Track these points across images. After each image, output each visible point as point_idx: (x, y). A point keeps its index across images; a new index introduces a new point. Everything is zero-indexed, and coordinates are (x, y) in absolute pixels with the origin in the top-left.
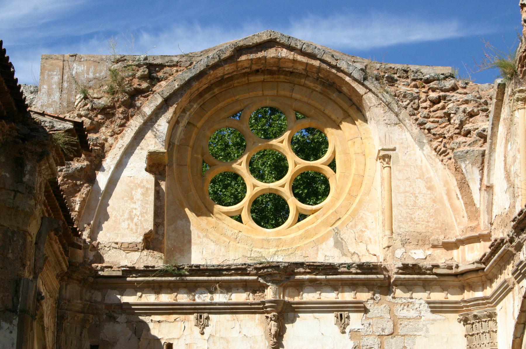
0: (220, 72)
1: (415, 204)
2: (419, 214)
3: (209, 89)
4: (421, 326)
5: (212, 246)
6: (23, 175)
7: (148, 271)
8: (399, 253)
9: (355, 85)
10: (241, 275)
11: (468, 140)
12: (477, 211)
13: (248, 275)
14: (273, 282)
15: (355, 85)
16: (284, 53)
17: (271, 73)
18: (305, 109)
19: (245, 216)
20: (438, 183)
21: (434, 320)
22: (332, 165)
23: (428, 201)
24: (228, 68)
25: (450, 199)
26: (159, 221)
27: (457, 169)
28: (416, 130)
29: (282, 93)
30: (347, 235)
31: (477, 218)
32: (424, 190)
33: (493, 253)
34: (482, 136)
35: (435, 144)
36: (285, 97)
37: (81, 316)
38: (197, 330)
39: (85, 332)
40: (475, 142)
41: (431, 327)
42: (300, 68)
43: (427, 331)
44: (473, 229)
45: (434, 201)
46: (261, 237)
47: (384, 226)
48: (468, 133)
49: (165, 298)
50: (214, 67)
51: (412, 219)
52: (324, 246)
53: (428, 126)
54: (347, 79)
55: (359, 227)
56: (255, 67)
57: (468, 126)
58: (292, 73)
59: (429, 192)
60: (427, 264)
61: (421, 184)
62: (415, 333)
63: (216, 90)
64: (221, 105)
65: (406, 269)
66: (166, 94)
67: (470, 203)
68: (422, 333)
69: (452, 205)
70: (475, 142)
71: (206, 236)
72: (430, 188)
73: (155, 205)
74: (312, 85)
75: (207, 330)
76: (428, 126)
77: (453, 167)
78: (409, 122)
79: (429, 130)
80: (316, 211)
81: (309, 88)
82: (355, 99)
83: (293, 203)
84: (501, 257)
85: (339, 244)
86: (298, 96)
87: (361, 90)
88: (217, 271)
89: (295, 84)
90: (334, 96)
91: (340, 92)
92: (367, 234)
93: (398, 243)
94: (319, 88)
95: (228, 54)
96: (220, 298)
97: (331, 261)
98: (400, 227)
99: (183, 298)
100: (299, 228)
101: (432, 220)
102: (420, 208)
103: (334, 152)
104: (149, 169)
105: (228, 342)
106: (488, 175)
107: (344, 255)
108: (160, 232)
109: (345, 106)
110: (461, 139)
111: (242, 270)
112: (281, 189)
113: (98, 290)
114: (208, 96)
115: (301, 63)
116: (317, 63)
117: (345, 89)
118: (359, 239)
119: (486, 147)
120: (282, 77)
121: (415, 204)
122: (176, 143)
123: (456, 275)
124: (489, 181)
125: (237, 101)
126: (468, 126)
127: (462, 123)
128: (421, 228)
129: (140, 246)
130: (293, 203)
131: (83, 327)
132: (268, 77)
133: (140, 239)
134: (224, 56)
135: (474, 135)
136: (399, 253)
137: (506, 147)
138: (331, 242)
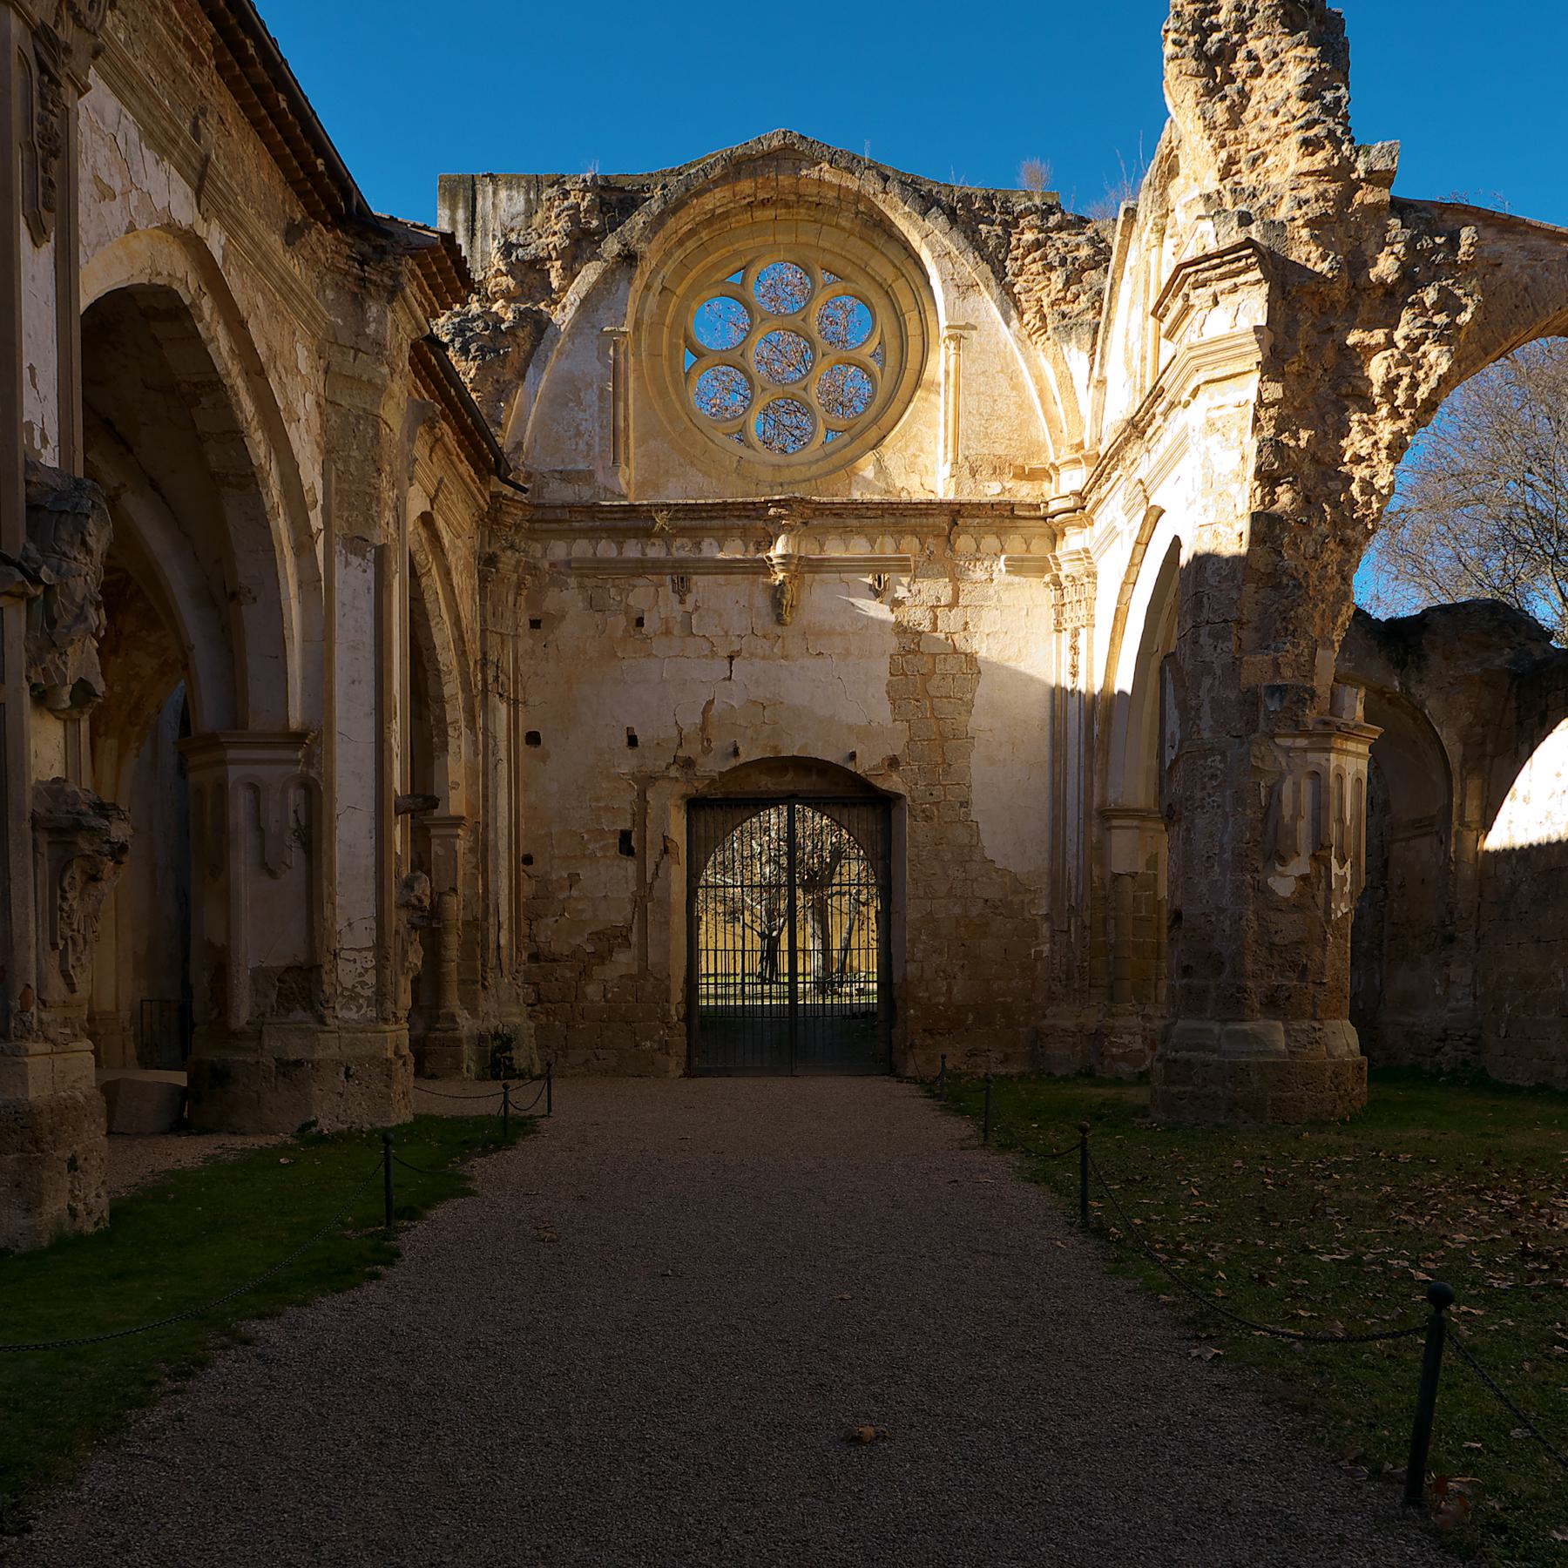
4: (991, 592)
21: (1009, 584)
23: (1012, 407)
25: (1043, 403)
29: (803, 239)
36: (807, 245)
38: (675, 598)
39: (522, 600)
41: (1004, 596)
43: (999, 600)
45: (1020, 407)
47: (946, 446)
59: (1014, 393)
62: (983, 603)
63: (704, 235)
64: (711, 259)
68: (993, 603)
69: (1046, 413)
71: (692, 464)
75: (690, 598)
81: (843, 229)
86: (828, 245)
89: (823, 224)
98: (968, 448)
101: (1016, 436)
106: (1102, 366)
113: (537, 540)
120: (803, 211)
124: (1100, 374)
125: (736, 252)
128: (999, 449)
131: (518, 594)
137: (1129, 314)
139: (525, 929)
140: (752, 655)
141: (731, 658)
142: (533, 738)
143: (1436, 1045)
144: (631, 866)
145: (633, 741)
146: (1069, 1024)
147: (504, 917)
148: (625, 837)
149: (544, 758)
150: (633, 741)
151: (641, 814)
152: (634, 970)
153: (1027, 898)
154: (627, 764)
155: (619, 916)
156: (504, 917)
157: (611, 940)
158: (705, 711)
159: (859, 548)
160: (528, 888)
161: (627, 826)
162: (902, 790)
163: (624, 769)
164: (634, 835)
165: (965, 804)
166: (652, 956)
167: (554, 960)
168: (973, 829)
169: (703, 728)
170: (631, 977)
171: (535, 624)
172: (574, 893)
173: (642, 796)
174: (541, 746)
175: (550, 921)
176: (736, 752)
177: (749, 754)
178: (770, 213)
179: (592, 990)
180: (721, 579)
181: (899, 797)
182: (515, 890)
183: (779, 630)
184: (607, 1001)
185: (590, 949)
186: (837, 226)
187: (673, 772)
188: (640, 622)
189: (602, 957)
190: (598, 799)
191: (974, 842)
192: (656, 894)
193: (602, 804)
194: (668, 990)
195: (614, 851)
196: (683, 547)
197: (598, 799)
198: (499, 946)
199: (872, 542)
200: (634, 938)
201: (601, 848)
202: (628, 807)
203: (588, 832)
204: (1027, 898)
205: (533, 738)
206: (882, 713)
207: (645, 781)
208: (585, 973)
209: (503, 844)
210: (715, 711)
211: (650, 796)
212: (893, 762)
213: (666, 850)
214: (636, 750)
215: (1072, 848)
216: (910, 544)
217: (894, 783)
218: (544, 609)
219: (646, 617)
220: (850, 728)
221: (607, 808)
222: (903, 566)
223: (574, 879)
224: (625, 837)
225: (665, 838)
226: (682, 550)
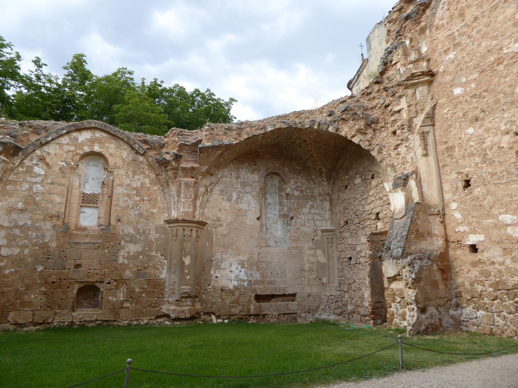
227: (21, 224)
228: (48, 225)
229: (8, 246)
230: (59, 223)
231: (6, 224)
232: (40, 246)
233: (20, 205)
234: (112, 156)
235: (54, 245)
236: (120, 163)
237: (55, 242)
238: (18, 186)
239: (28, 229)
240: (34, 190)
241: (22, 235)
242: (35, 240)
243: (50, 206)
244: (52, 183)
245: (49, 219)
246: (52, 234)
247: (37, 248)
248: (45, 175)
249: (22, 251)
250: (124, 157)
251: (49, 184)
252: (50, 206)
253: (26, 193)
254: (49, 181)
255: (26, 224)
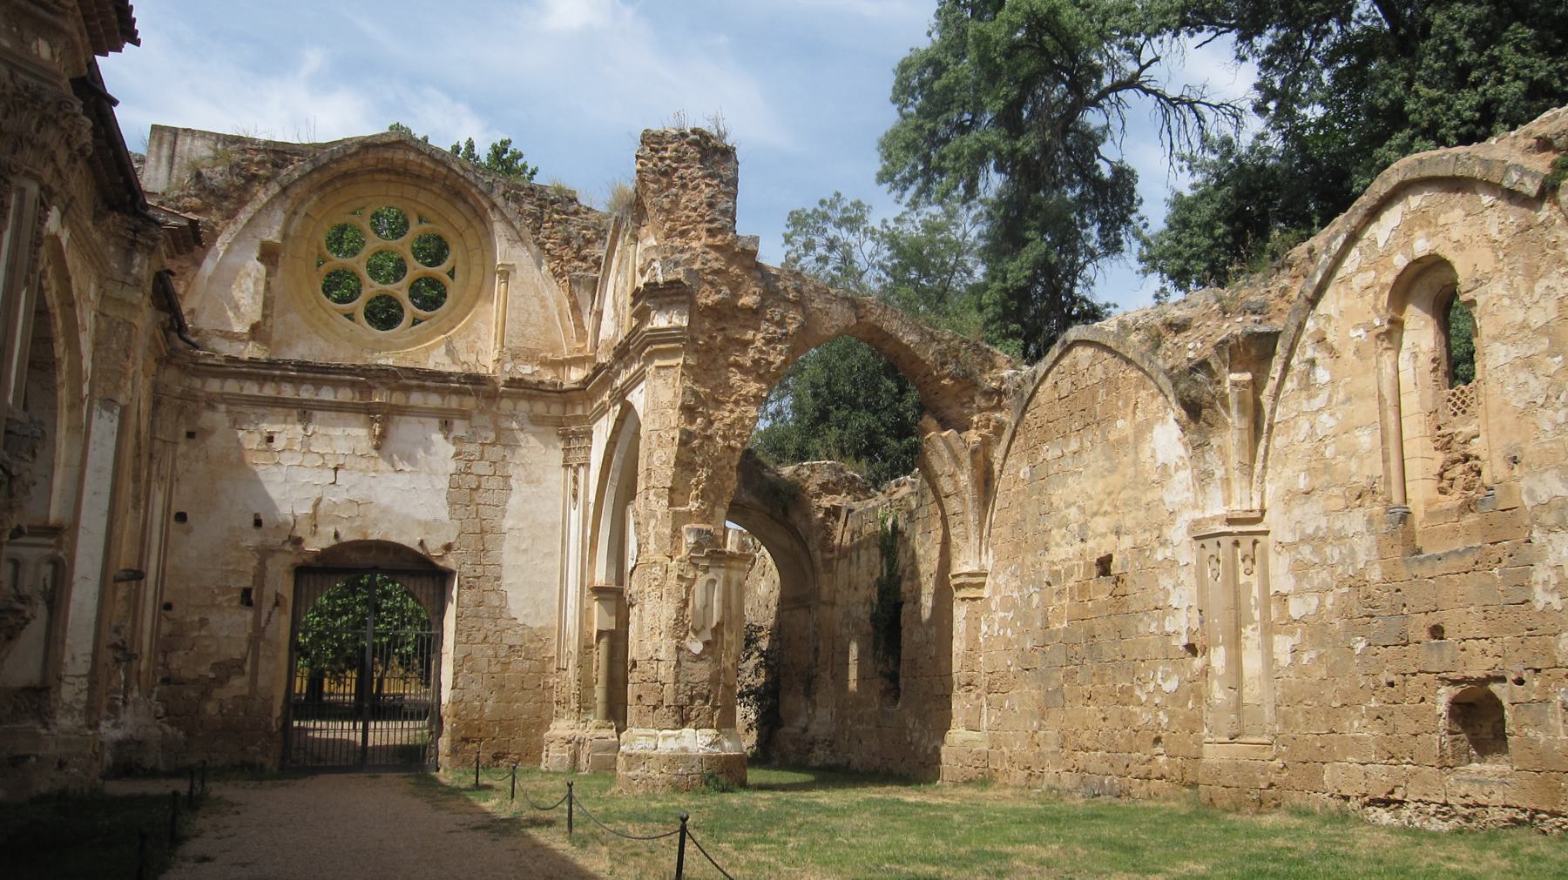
0: (344, 167)
1: (528, 321)
2: (530, 330)
3: (331, 182)
5: (321, 343)
6: (131, 266)
7: (253, 362)
8: (508, 367)
9: (479, 197)
10: (350, 374)
11: (584, 265)
12: (585, 333)
13: (356, 375)
14: (382, 383)
15: (479, 197)
16: (412, 156)
17: (398, 173)
18: (429, 214)
19: (360, 316)
20: (551, 303)
22: (452, 274)
24: (352, 164)
25: (561, 320)
26: (268, 312)
27: (571, 294)
28: (534, 248)
30: (460, 344)
31: (585, 340)
32: (538, 309)
33: (595, 375)
34: (597, 263)
35: (553, 265)
37: (179, 402)
40: (591, 268)
42: (427, 173)
44: (579, 350)
45: (546, 320)
46: (371, 338)
48: (584, 259)
49: (269, 390)
50: (338, 161)
51: (523, 335)
52: (435, 352)
53: (547, 246)
54: (473, 190)
55: (471, 338)
56: (380, 166)
57: (584, 252)
58: (418, 176)
60: (534, 379)
61: (535, 301)
63: (338, 185)
65: (512, 382)
66: (285, 183)
67: (580, 325)
70: (591, 268)
71: (317, 332)
72: (544, 307)
73: (265, 297)
74: (438, 191)
76: (547, 246)
77: (567, 289)
78: (530, 239)
79: (549, 250)
80: (430, 317)
82: (480, 211)
83: (410, 308)
84: (602, 380)
85: (450, 352)
87: (486, 205)
88: (326, 369)
90: (461, 206)
91: (466, 202)
92: (480, 345)
93: (508, 357)
94: (445, 195)
95: (353, 150)
96: (327, 395)
97: (441, 368)
99: (288, 391)
100: (412, 333)
102: (532, 325)
103: (455, 260)
104: (261, 259)
105: (331, 439)
107: (454, 363)
108: (268, 324)
109: (470, 216)
110: (576, 263)
111: (350, 370)
112: (399, 293)
114: (329, 189)
115: (429, 168)
116: (444, 171)
117: (471, 200)
118: (471, 349)
119: (599, 275)
121: (528, 321)
122: (292, 233)
123: (559, 392)
126: (584, 252)
127: (580, 249)
128: (531, 345)
129: (246, 337)
130: (410, 308)
132: (393, 177)
133: (246, 329)
134: (349, 152)
135: (590, 263)
136: (508, 367)
138: (443, 349)
139: (161, 659)
140: (352, 468)
141: (336, 469)
142: (181, 517)
143: (808, 747)
144: (249, 615)
145: (258, 523)
146: (567, 733)
147: (146, 648)
148: (246, 593)
149: (188, 532)
150: (258, 523)
151: (261, 575)
152: (246, 691)
153: (541, 644)
154: (253, 539)
155: (236, 651)
156: (146, 648)
157: (235, 667)
158: (316, 505)
159: (434, 401)
160: (166, 628)
161: (248, 583)
162: (453, 567)
163: (250, 543)
164: (254, 592)
165: (498, 579)
166: (262, 682)
167: (182, 683)
168: (504, 598)
169: (314, 516)
170: (243, 697)
171: (191, 435)
172: (203, 633)
173: (262, 563)
174: (185, 525)
175: (181, 653)
176: (336, 535)
177: (346, 536)
178: (386, 177)
179: (211, 708)
180: (333, 414)
181: (451, 573)
182: (156, 630)
183: (374, 453)
184: (223, 715)
185: (212, 675)
186: (430, 191)
187: (288, 547)
188: (270, 439)
189: (221, 681)
190: (228, 564)
191: (503, 604)
192: (268, 635)
193: (231, 568)
194: (271, 708)
195: (235, 603)
196: (307, 390)
197: (228, 564)
198: (139, 672)
199: (443, 399)
200: (248, 668)
201: (230, 600)
202: (251, 571)
203: (218, 587)
204: (541, 644)
205: (181, 517)
206: (444, 514)
207: (265, 553)
208: (206, 695)
209: (150, 594)
210: (321, 505)
211: (269, 562)
212: (448, 547)
213: (277, 604)
214: (261, 530)
215: (570, 612)
216: (470, 403)
217: (450, 562)
218: (199, 423)
219: (276, 436)
220: (420, 523)
221: (234, 571)
222: (465, 415)
223: (203, 622)
224: (246, 593)
225: (277, 594)
226: (306, 393)
227: (1310, 531)
228: (1355, 522)
229: (1300, 593)
230: (1378, 509)
231: (1288, 538)
232: (1352, 581)
233: (1302, 483)
234: (1462, 249)
235: (1375, 575)
236: (1484, 259)
237: (1377, 566)
238: (1292, 432)
239: (1323, 539)
240: (1318, 431)
241: (1317, 560)
242: (1340, 570)
243: (1353, 465)
244: (1348, 400)
245: (1358, 502)
246: (1368, 544)
247: (1346, 589)
248: (1332, 382)
249: (1321, 604)
250: (1493, 232)
251: (1343, 403)
252: (1353, 465)
253: (1307, 445)
254: (1341, 396)
255: (1318, 528)
